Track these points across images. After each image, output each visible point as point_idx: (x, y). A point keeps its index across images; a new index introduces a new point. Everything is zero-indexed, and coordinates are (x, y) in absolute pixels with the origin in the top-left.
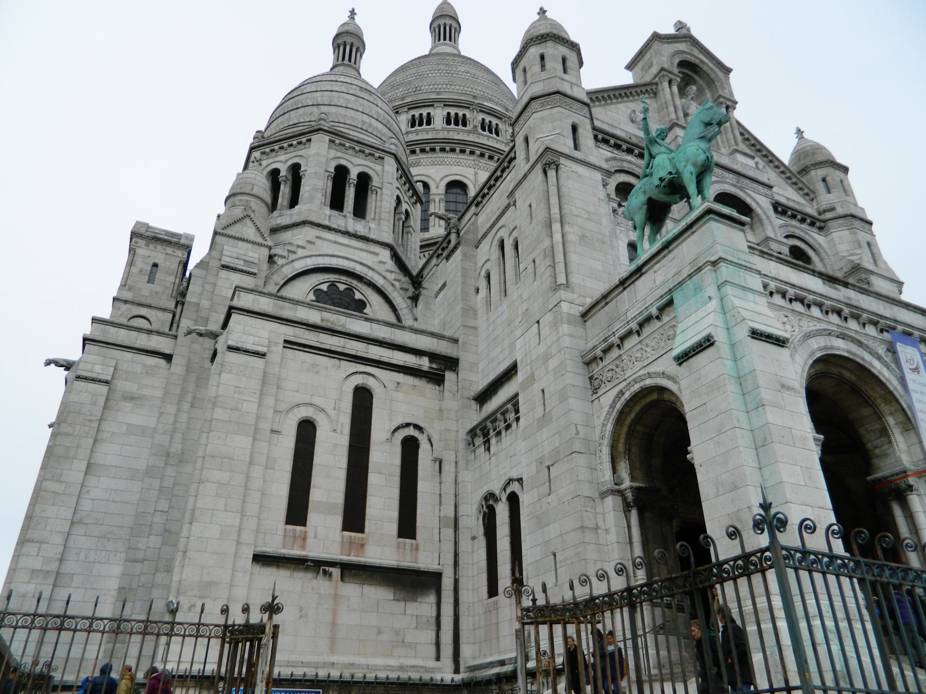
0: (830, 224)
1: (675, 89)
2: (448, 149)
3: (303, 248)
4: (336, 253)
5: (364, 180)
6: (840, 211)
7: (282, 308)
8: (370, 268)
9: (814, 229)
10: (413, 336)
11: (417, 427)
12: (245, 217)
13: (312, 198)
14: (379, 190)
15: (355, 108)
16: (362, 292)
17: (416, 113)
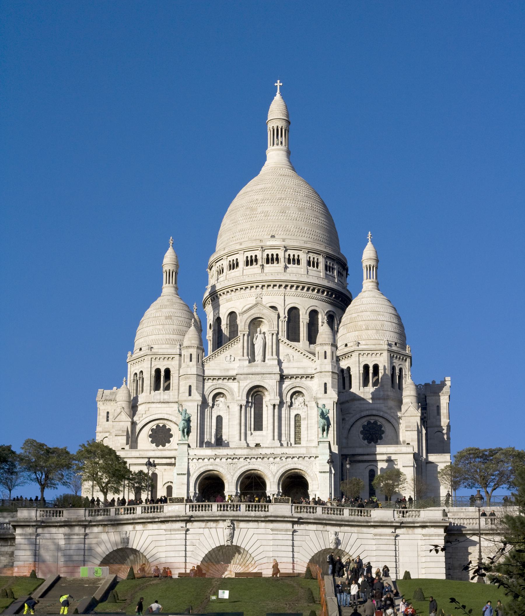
0: (315, 375)
1: (246, 337)
2: (244, 288)
3: (145, 414)
4: (157, 412)
5: (168, 372)
6: (318, 370)
7: (127, 454)
8: (170, 414)
9: (309, 379)
10: (169, 452)
11: (172, 482)
12: (121, 412)
13: (147, 390)
14: (173, 375)
15: (162, 333)
16: (169, 425)
17: (230, 258)
